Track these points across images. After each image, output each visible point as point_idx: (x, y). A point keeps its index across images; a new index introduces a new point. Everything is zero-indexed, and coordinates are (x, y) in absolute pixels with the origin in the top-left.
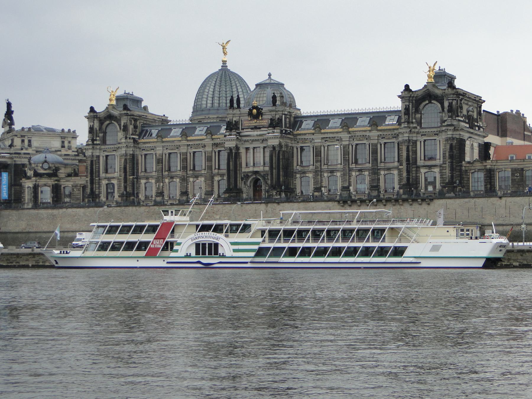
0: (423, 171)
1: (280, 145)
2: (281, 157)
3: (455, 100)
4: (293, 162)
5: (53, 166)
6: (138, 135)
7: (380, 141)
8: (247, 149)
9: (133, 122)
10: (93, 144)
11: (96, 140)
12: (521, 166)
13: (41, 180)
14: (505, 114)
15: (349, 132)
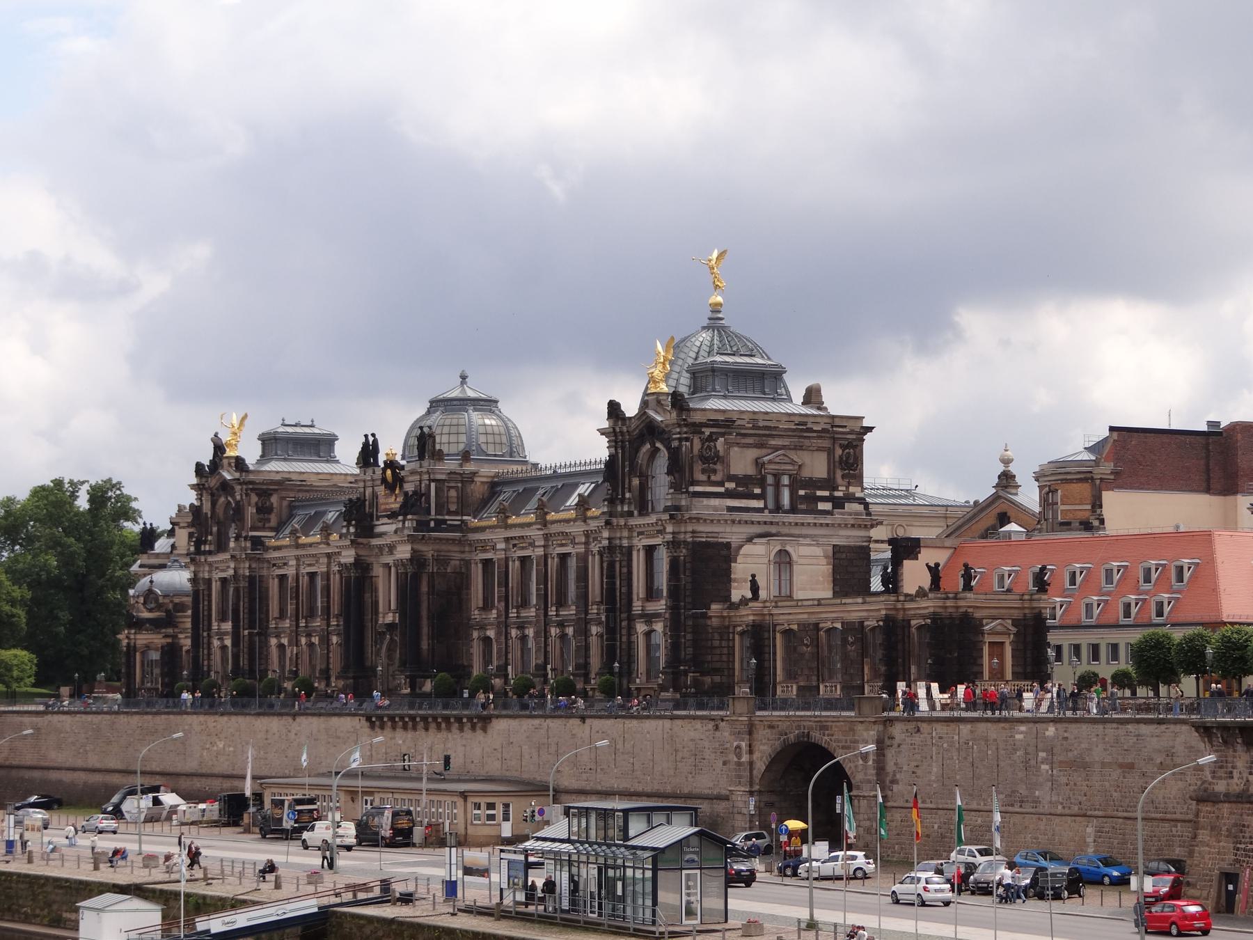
0: (641, 628)
1: (417, 560)
2: (424, 588)
3: (687, 439)
4: (469, 600)
5: (167, 601)
6: (272, 529)
7: (550, 550)
8: (387, 566)
9: (254, 498)
10: (198, 551)
11: (205, 542)
12: (813, 619)
13: (138, 636)
14: (1234, 427)
15: (545, 524)
